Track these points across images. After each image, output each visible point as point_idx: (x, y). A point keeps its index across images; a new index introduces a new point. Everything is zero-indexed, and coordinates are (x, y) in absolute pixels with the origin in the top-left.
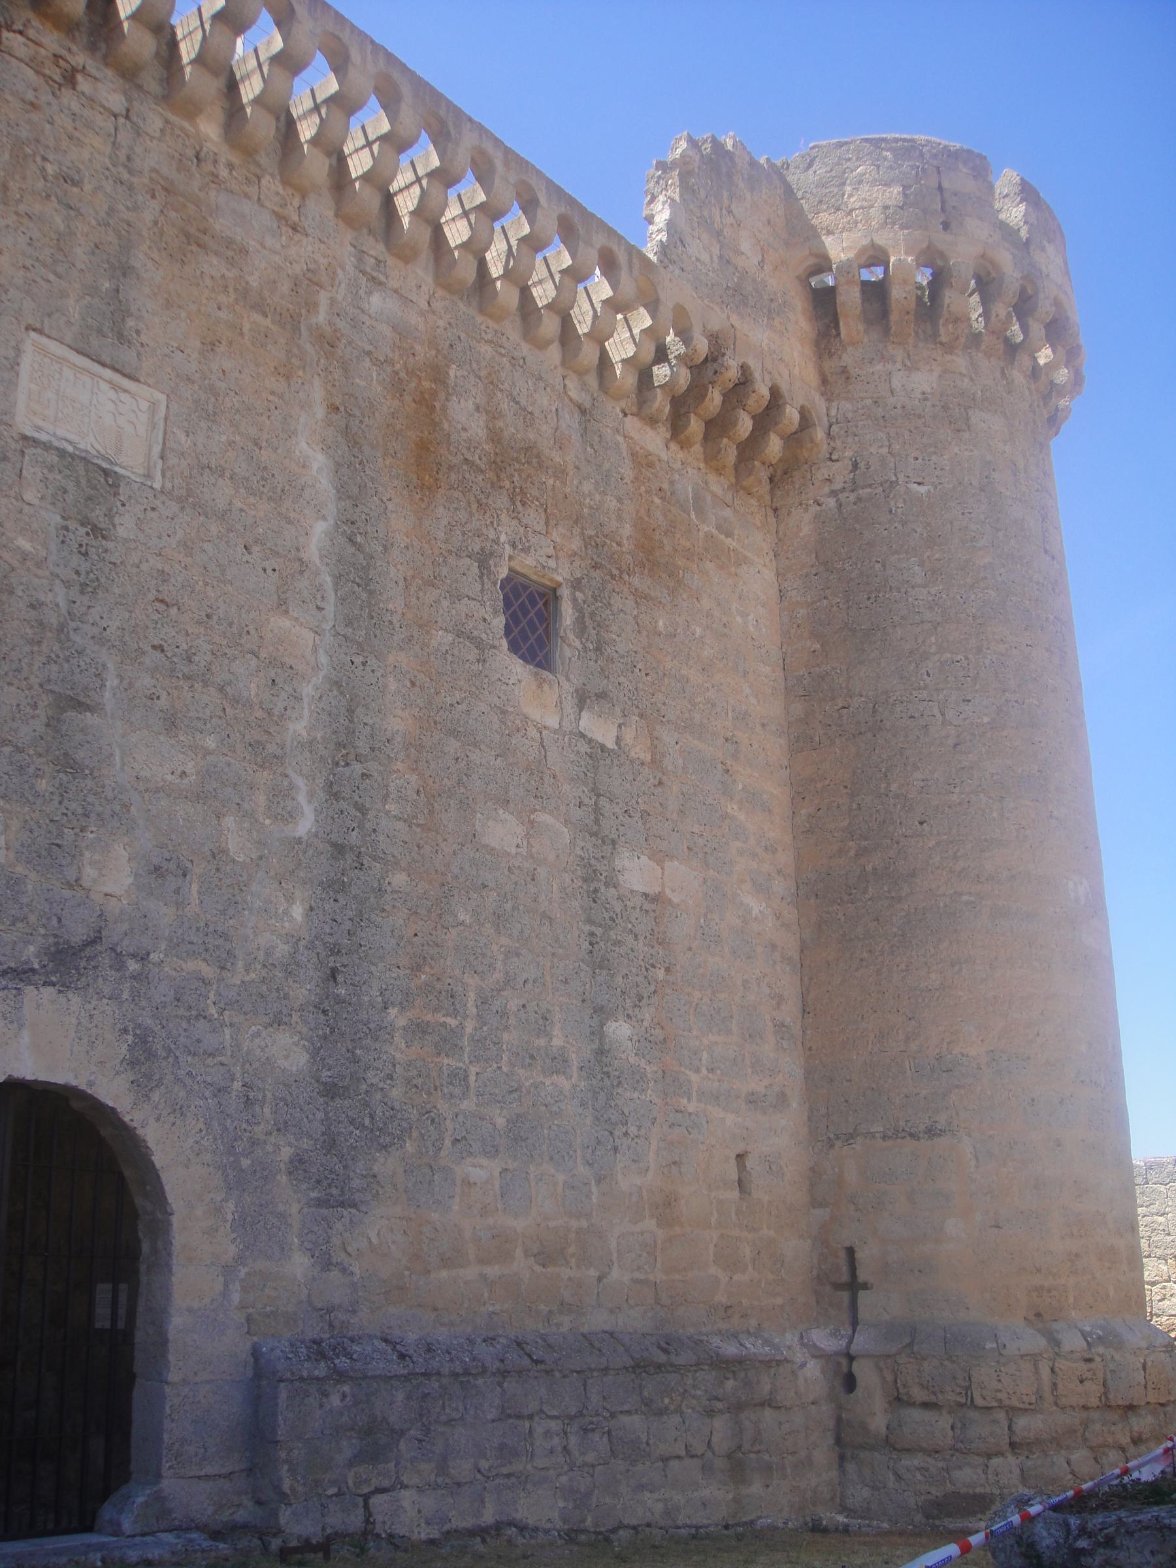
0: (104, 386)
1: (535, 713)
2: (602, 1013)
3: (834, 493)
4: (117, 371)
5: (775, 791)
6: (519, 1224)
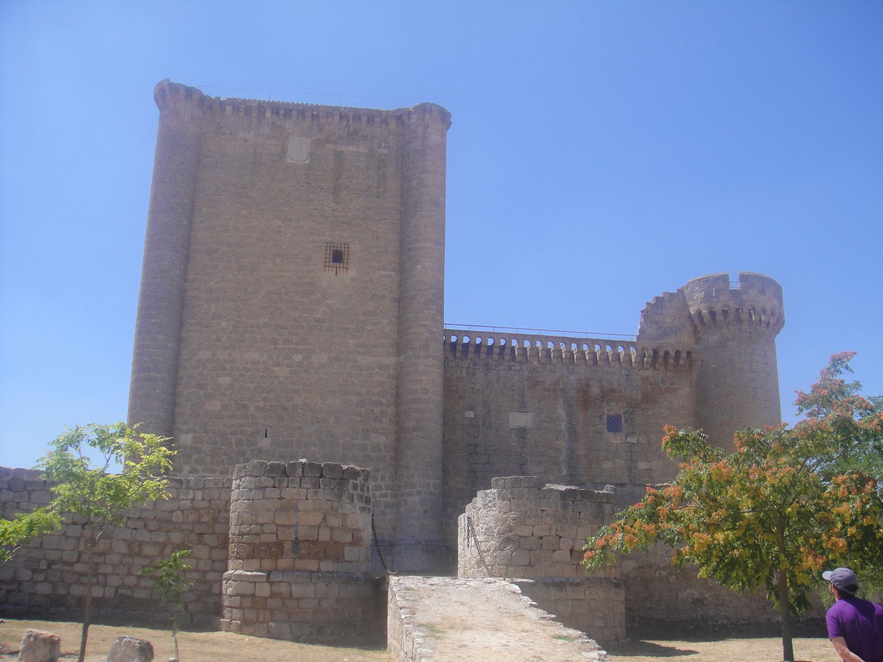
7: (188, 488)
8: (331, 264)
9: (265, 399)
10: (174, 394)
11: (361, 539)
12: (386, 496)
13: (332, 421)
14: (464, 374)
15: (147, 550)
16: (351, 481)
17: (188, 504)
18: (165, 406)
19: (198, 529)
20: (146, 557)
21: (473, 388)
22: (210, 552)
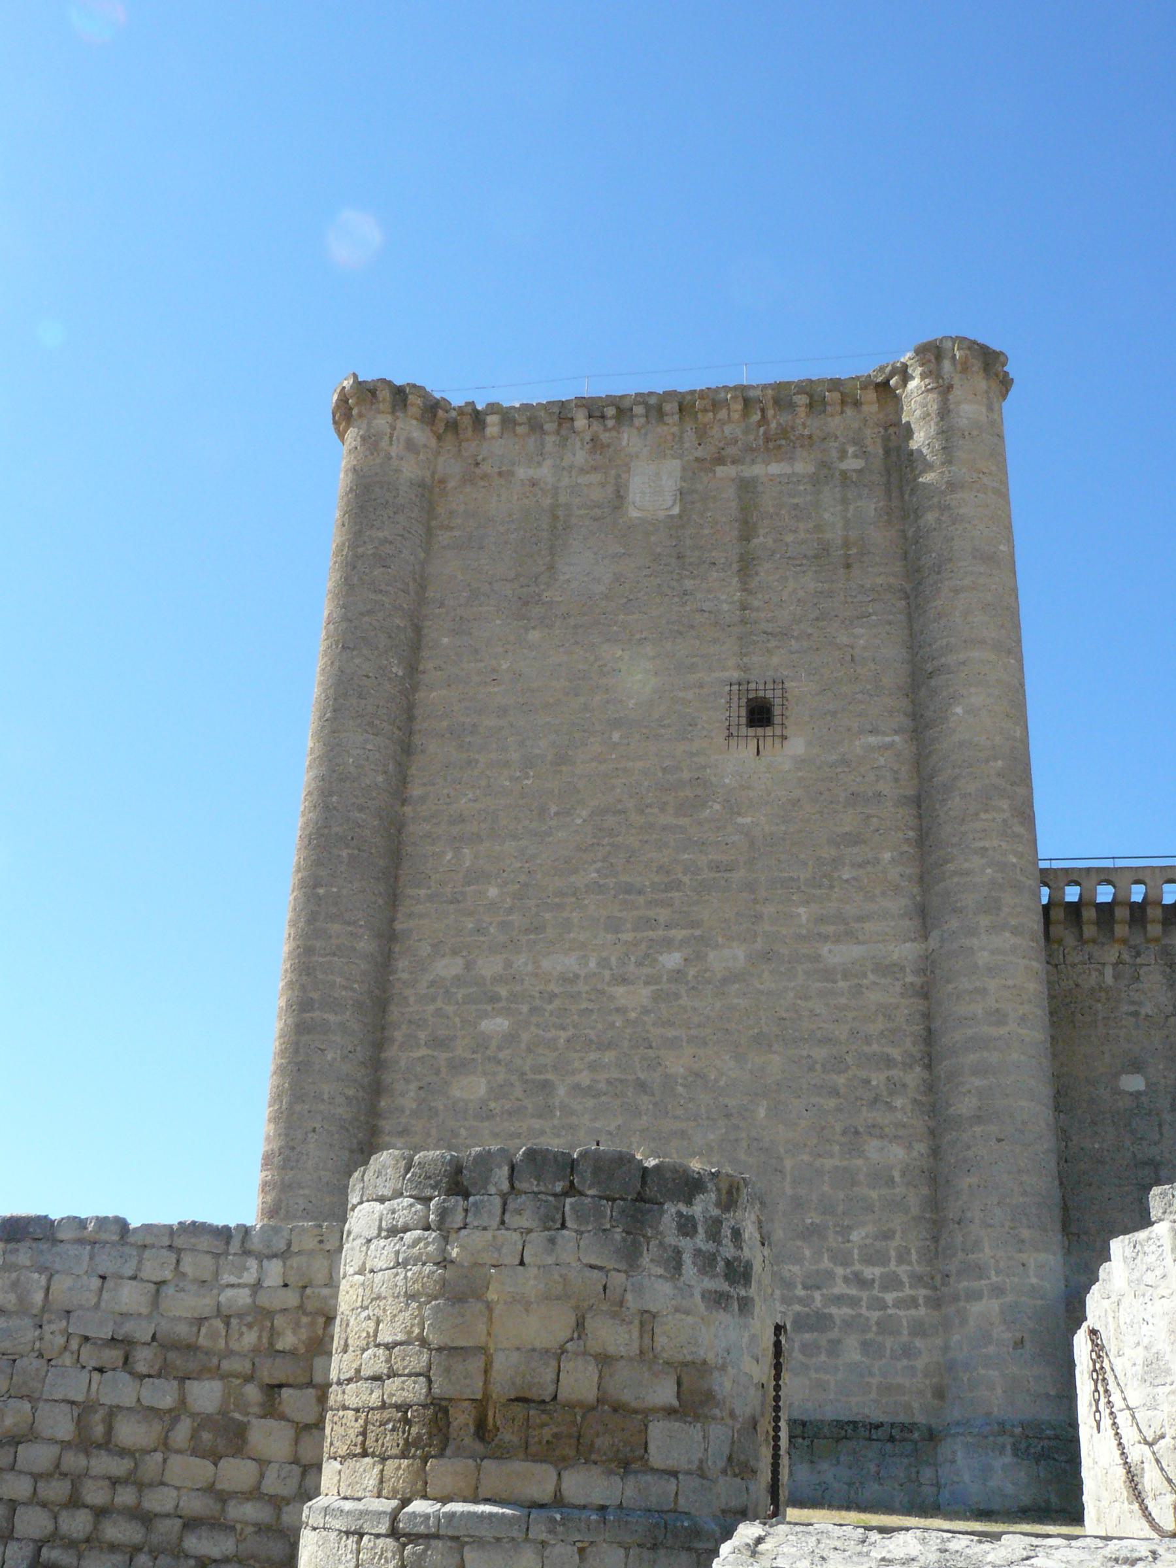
7: (246, 1253)
8: (744, 730)
9: (593, 1067)
10: (376, 1064)
11: (709, 1397)
12: (913, 1302)
13: (762, 1112)
14: (1109, 980)
15: (129, 1432)
16: (671, 1209)
17: (243, 1297)
18: (350, 1092)
19: (271, 1371)
20: (123, 1452)
21: (1136, 1014)
22: (297, 1441)
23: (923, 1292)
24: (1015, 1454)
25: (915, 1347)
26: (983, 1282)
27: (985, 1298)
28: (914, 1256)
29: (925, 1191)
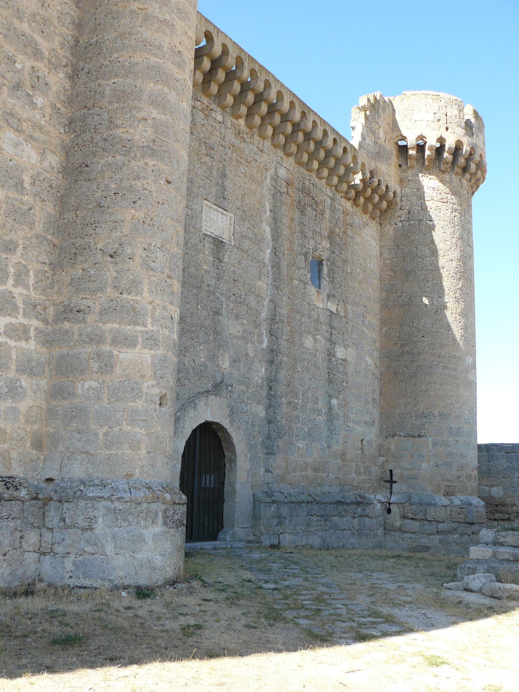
0: (220, 214)
1: (317, 303)
2: (330, 397)
3: (401, 221)
4: (222, 209)
5: (376, 322)
6: (310, 460)
23: (35, 323)
24: (165, 524)
25: (21, 387)
26: (139, 328)
27: (139, 346)
28: (31, 281)
29: (50, 208)
